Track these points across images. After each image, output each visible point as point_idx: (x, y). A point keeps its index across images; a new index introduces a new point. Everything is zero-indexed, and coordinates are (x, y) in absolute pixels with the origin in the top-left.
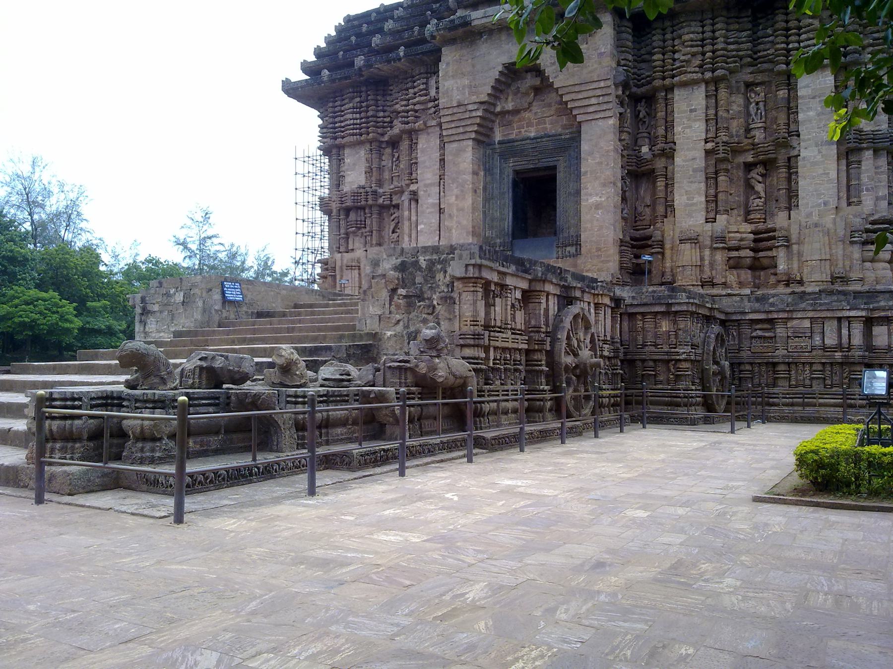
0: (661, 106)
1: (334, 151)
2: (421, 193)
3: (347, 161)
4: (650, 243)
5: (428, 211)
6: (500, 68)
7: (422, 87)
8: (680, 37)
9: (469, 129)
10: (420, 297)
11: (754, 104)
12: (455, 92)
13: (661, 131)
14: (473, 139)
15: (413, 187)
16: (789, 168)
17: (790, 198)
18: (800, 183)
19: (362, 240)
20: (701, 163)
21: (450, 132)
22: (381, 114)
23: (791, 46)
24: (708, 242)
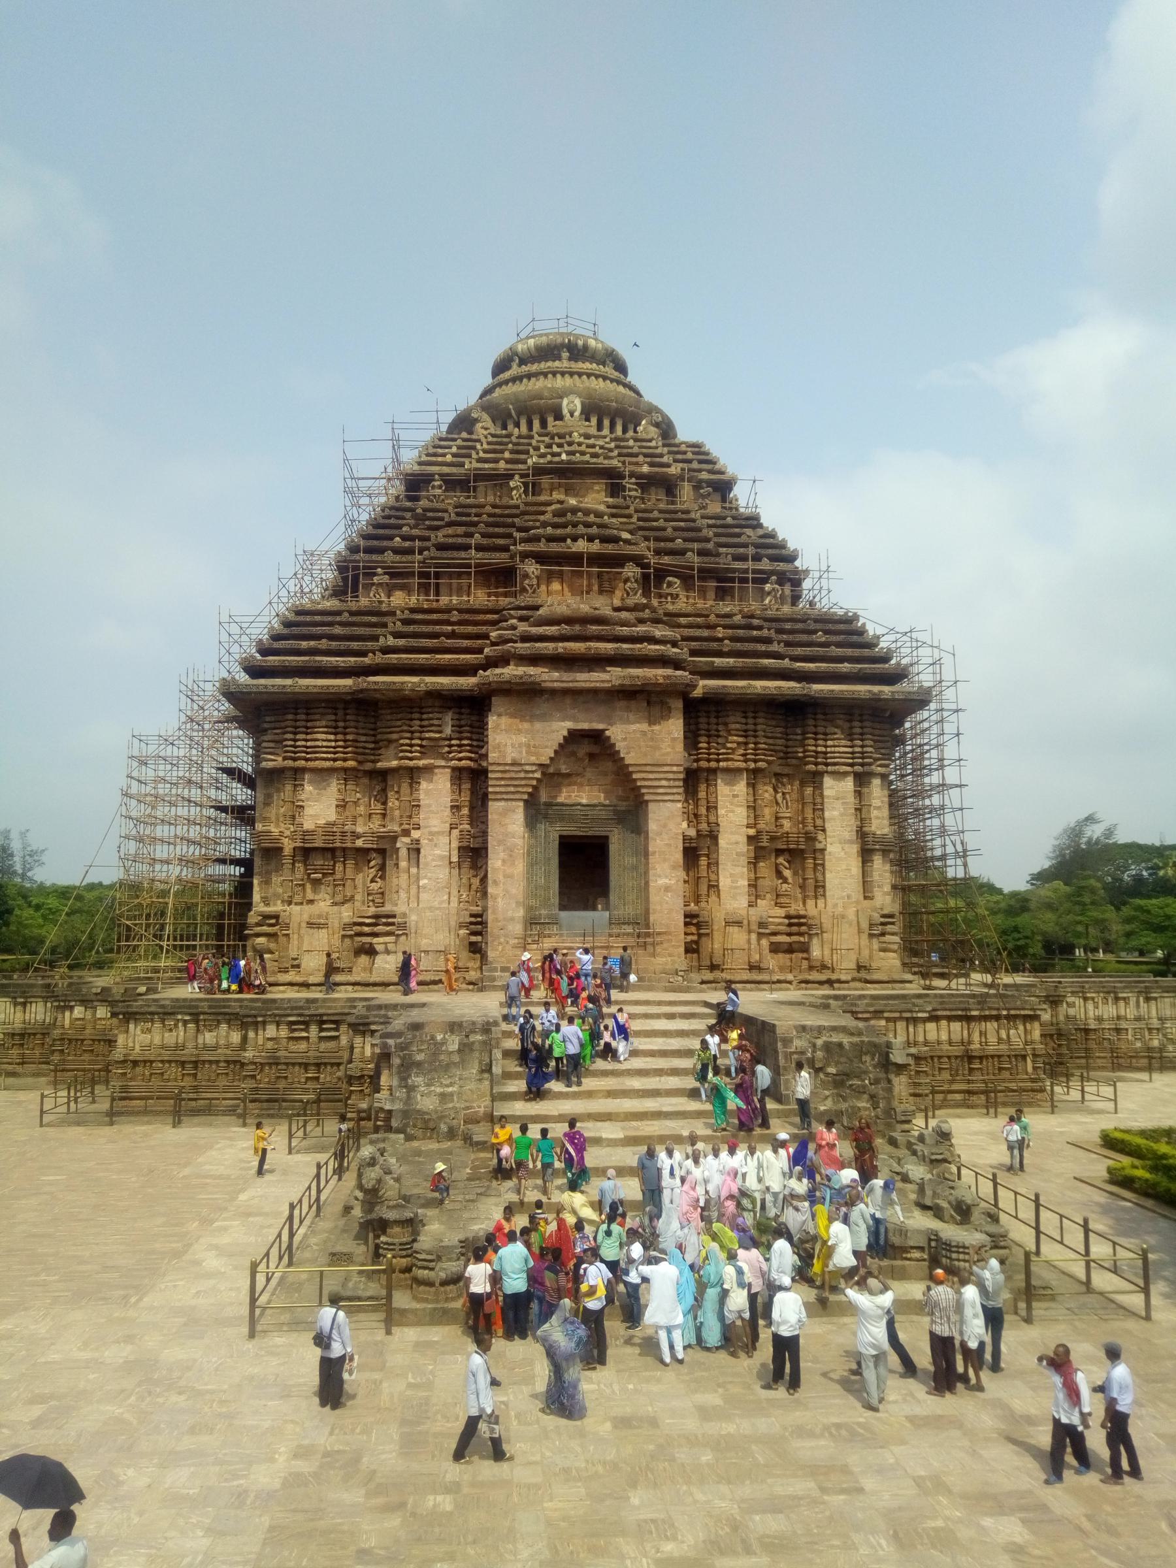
0: (703, 787)
1: (289, 774)
2: (424, 842)
3: (308, 788)
4: (695, 921)
5: (434, 863)
6: (565, 733)
7: (436, 722)
8: (726, 724)
9: (520, 789)
10: (848, 1075)
11: (779, 796)
12: (509, 749)
13: (703, 811)
14: (526, 801)
15: (415, 834)
16: (815, 859)
17: (816, 887)
18: (828, 875)
19: (330, 890)
20: (744, 847)
21: (498, 789)
22: (363, 738)
23: (819, 749)
24: (754, 927)
